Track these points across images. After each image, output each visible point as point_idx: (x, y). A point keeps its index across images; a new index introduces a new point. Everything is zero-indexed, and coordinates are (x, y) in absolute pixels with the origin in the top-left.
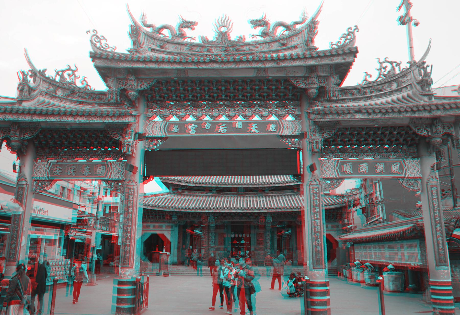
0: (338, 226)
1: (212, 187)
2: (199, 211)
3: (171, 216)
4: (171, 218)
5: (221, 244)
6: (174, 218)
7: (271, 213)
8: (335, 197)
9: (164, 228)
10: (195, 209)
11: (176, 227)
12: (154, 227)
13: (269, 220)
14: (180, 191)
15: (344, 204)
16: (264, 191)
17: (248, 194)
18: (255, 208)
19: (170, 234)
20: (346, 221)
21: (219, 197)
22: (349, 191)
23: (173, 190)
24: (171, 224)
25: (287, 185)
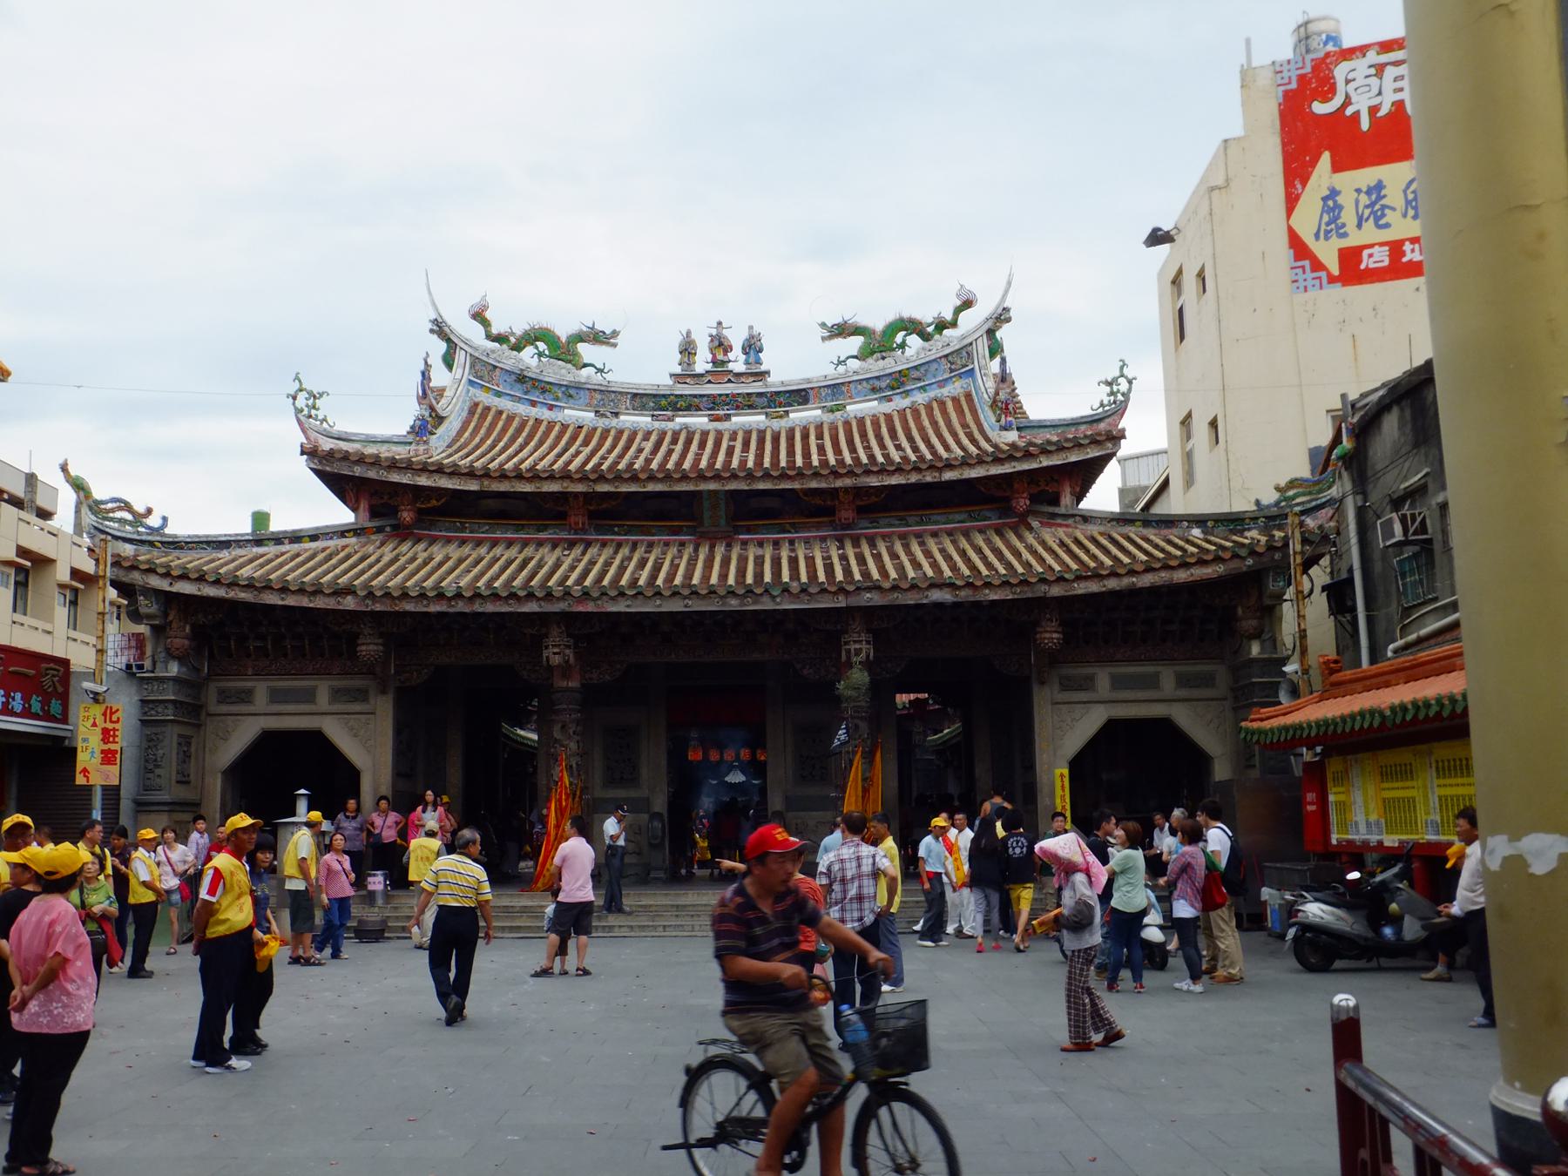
0: (1207, 681)
1: (562, 497)
2: (490, 608)
3: (353, 640)
4: (353, 655)
5: (611, 781)
6: (369, 648)
7: (869, 612)
8: (1196, 532)
9: (323, 700)
10: (471, 599)
11: (384, 692)
12: (276, 696)
13: (858, 652)
14: (407, 516)
15: (1250, 562)
16: (829, 512)
17: (749, 531)
18: (786, 590)
19: (366, 742)
20: (1255, 650)
21: (604, 544)
22: (1269, 497)
23: (374, 513)
24: (357, 682)
25: (948, 476)
